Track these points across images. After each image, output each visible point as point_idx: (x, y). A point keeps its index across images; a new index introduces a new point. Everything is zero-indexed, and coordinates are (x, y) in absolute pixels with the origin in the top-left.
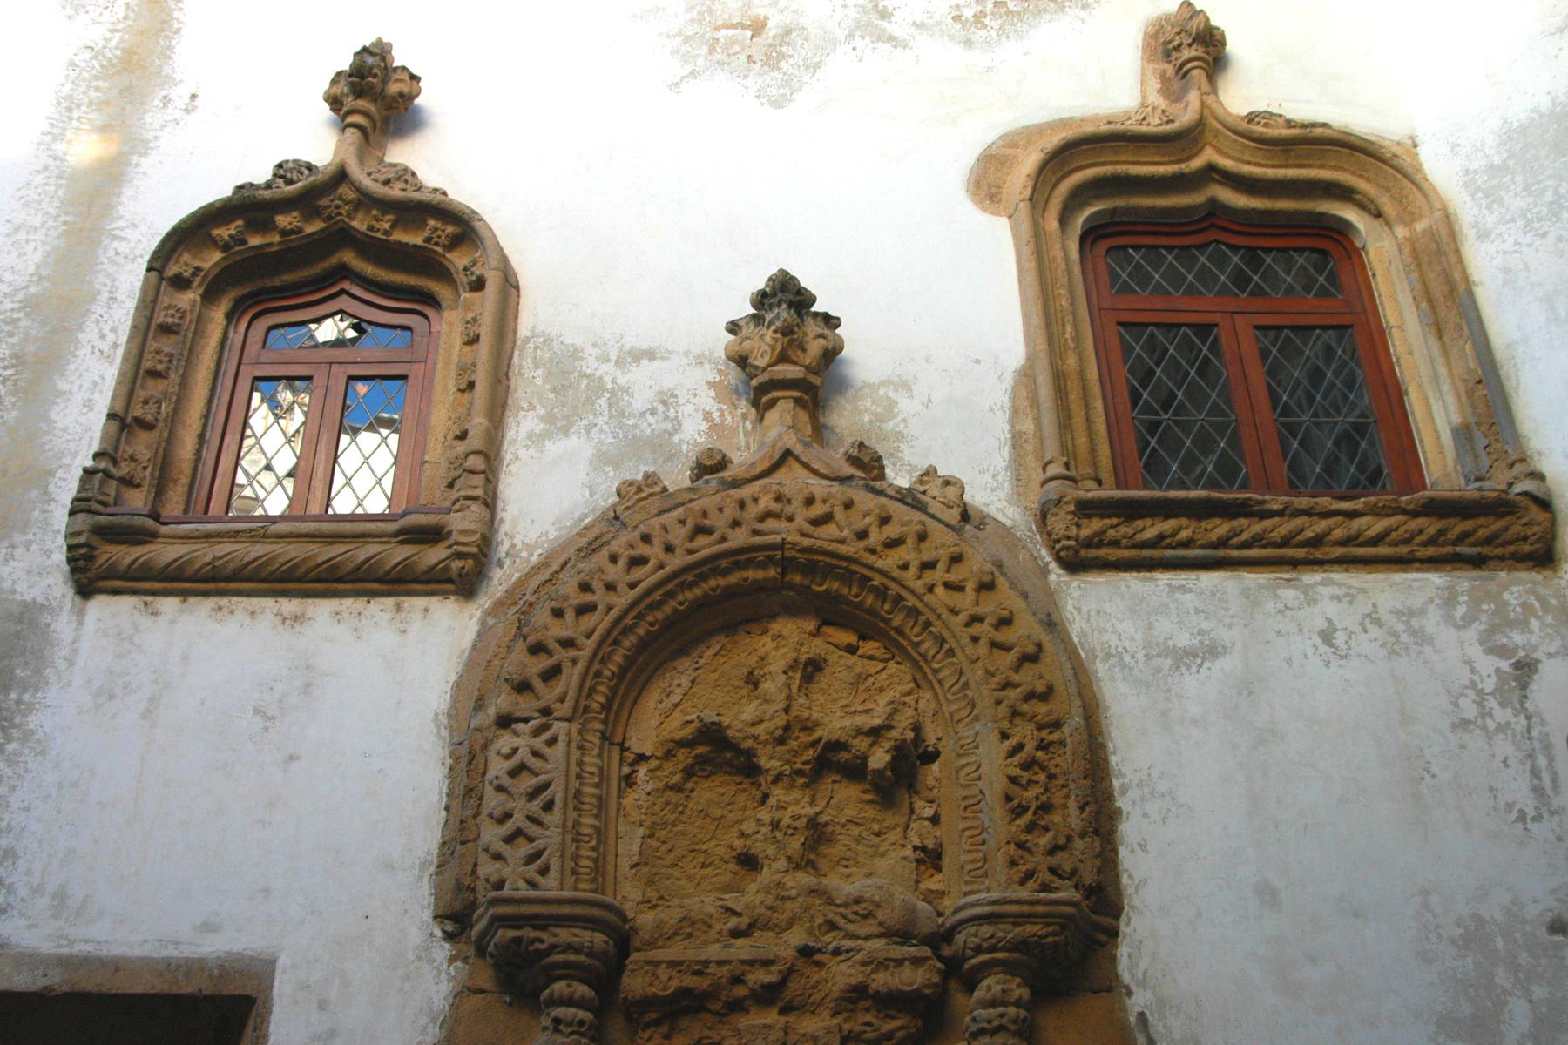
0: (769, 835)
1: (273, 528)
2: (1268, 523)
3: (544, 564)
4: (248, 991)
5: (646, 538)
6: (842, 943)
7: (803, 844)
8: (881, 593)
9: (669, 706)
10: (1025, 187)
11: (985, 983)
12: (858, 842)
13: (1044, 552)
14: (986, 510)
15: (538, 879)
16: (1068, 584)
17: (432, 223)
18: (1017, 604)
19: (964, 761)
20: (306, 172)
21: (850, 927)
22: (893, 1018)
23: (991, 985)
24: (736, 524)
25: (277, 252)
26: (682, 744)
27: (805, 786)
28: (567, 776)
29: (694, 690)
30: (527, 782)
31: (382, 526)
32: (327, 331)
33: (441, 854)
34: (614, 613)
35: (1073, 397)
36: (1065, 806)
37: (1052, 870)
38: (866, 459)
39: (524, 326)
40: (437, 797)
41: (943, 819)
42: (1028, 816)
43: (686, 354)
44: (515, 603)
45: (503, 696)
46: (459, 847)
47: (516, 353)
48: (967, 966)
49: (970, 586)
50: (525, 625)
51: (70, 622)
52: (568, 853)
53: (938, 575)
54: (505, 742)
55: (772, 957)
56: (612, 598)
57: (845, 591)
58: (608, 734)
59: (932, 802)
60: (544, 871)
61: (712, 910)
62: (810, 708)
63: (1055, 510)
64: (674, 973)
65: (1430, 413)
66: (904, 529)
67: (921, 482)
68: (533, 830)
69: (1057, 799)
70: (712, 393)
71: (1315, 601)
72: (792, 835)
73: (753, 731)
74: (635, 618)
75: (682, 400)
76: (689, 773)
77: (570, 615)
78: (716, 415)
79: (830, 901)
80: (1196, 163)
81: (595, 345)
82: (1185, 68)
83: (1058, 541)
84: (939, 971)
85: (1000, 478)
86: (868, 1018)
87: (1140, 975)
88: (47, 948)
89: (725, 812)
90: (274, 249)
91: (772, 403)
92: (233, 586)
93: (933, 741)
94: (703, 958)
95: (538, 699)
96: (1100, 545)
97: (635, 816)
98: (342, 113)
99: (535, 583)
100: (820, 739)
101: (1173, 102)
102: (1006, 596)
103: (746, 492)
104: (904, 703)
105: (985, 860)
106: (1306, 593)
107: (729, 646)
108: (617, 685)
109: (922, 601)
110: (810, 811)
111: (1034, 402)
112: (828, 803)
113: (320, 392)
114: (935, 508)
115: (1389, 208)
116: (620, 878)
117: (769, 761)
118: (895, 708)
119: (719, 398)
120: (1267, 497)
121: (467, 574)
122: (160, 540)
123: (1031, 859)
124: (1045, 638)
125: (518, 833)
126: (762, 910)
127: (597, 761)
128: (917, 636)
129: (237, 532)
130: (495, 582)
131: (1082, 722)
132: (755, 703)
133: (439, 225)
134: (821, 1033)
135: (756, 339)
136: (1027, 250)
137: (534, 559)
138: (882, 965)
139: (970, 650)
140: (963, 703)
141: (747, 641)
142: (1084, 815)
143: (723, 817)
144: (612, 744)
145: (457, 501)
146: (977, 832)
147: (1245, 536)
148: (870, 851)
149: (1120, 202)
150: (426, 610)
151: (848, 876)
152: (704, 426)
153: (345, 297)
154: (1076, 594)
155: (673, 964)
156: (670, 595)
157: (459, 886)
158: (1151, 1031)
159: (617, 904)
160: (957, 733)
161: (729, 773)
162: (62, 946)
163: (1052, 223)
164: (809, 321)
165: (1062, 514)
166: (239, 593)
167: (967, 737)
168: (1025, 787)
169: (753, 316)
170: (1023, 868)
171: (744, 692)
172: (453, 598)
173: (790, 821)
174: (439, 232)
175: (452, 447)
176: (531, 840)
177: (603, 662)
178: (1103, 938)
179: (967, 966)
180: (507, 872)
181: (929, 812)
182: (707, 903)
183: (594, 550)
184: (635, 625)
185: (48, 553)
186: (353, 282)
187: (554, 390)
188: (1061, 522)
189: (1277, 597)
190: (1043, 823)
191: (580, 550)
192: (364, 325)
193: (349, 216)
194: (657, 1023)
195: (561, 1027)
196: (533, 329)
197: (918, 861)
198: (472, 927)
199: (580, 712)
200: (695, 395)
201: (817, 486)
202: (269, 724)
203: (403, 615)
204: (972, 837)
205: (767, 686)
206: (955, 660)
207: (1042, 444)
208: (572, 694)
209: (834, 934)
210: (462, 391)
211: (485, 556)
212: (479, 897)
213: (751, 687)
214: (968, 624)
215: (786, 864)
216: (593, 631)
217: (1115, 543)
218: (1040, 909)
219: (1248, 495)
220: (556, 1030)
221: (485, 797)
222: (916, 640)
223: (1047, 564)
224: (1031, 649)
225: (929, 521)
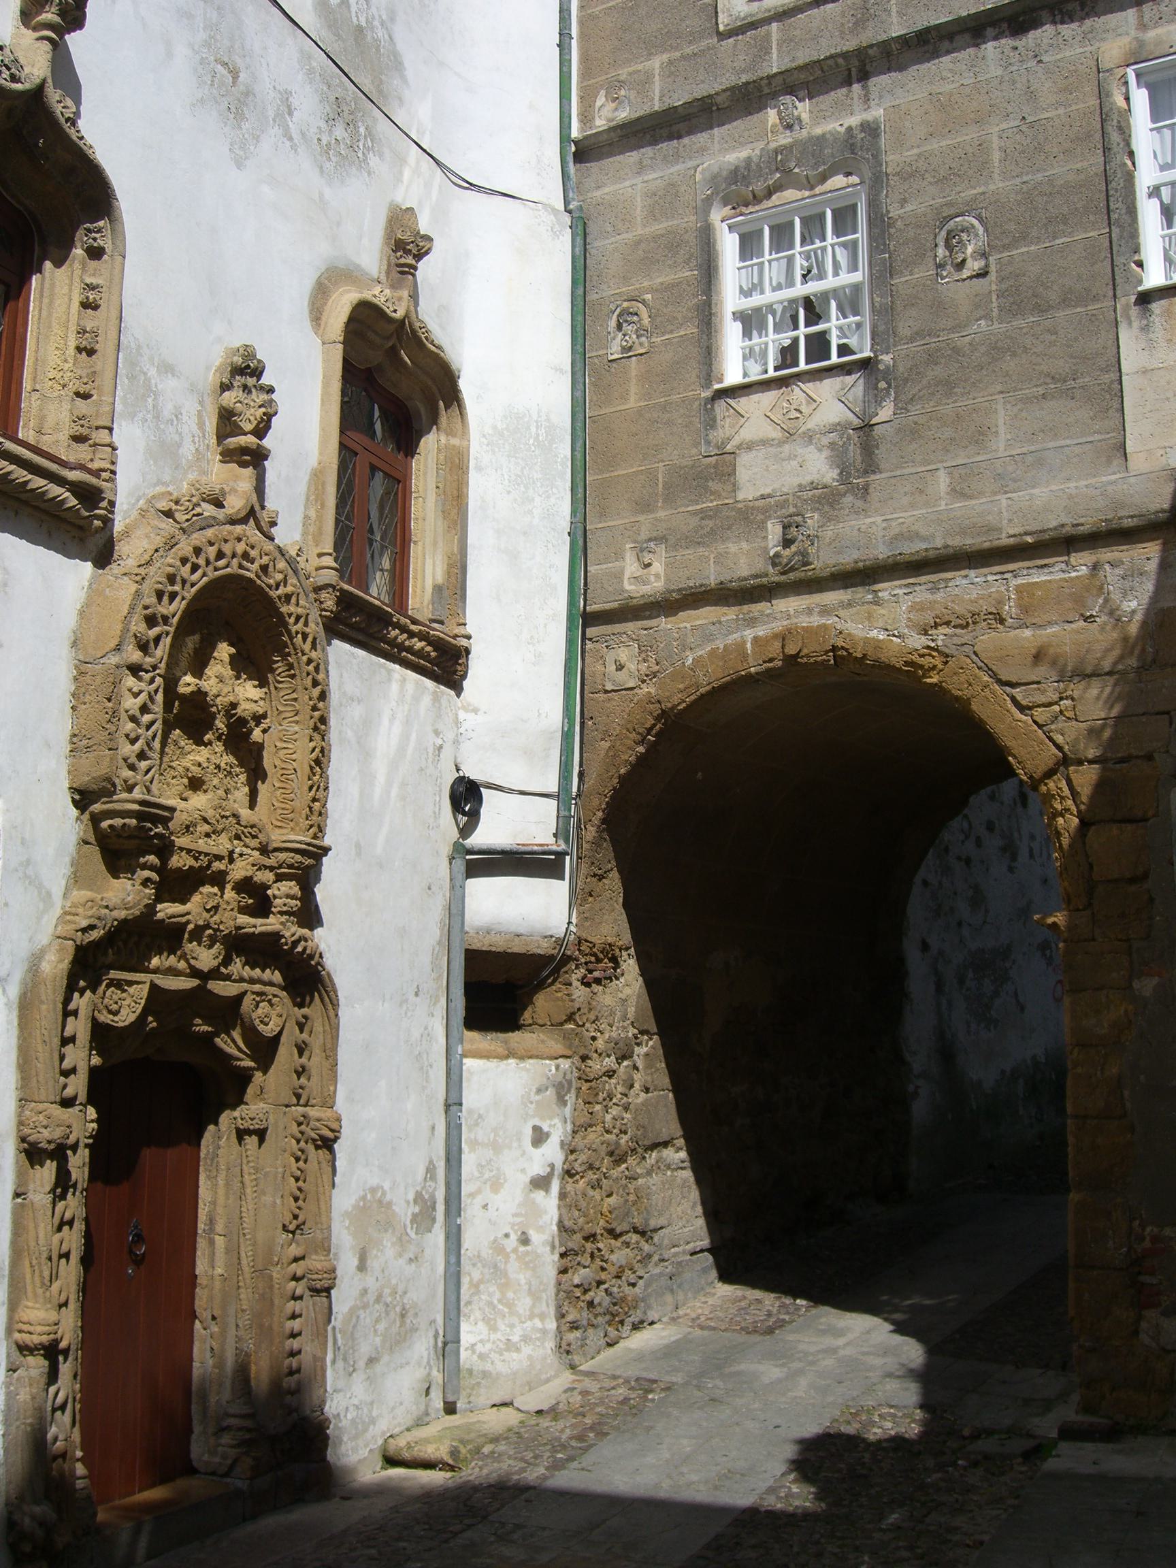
78: (197, 439)
79: (238, 823)
155: (189, 851)
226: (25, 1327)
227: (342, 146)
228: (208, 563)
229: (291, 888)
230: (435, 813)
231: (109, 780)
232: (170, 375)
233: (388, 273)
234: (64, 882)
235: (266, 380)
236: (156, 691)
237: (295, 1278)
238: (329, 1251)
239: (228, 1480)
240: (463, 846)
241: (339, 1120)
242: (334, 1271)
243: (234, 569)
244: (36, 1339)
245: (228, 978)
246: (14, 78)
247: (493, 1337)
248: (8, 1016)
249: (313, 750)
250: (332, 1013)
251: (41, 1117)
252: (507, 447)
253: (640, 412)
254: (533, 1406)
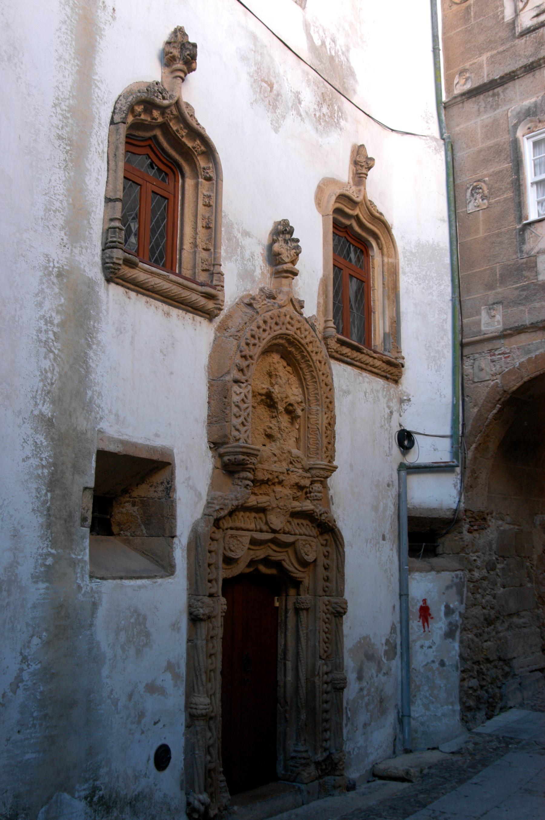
4: (170, 461)
8: (303, 357)
17: (198, 142)
51: (104, 293)
57: (295, 352)
65: (379, 323)
80: (356, 213)
88: (116, 436)
90: (147, 123)
92: (154, 295)
114: (317, 332)
115: (385, 250)
122: (138, 268)
133: (200, 144)
134: (289, 495)
152: (260, 272)
155: (267, 470)
162: (119, 435)
185: (93, 255)
195: (248, 487)
226: (194, 706)
227: (326, 117)
228: (271, 328)
229: (318, 488)
230: (389, 448)
231: (226, 436)
232: (248, 237)
233: (353, 178)
234: (207, 489)
235: (294, 236)
236: (248, 392)
237: (327, 683)
238: (343, 669)
239: (294, 784)
240: (405, 464)
241: (346, 603)
242: (345, 679)
243: (284, 331)
244: (199, 712)
245: (288, 533)
246: (164, 98)
247: (428, 713)
248: (182, 553)
249: (328, 417)
250: (341, 549)
251: (200, 603)
252: (418, 261)
253: (485, 238)
254: (448, 749)
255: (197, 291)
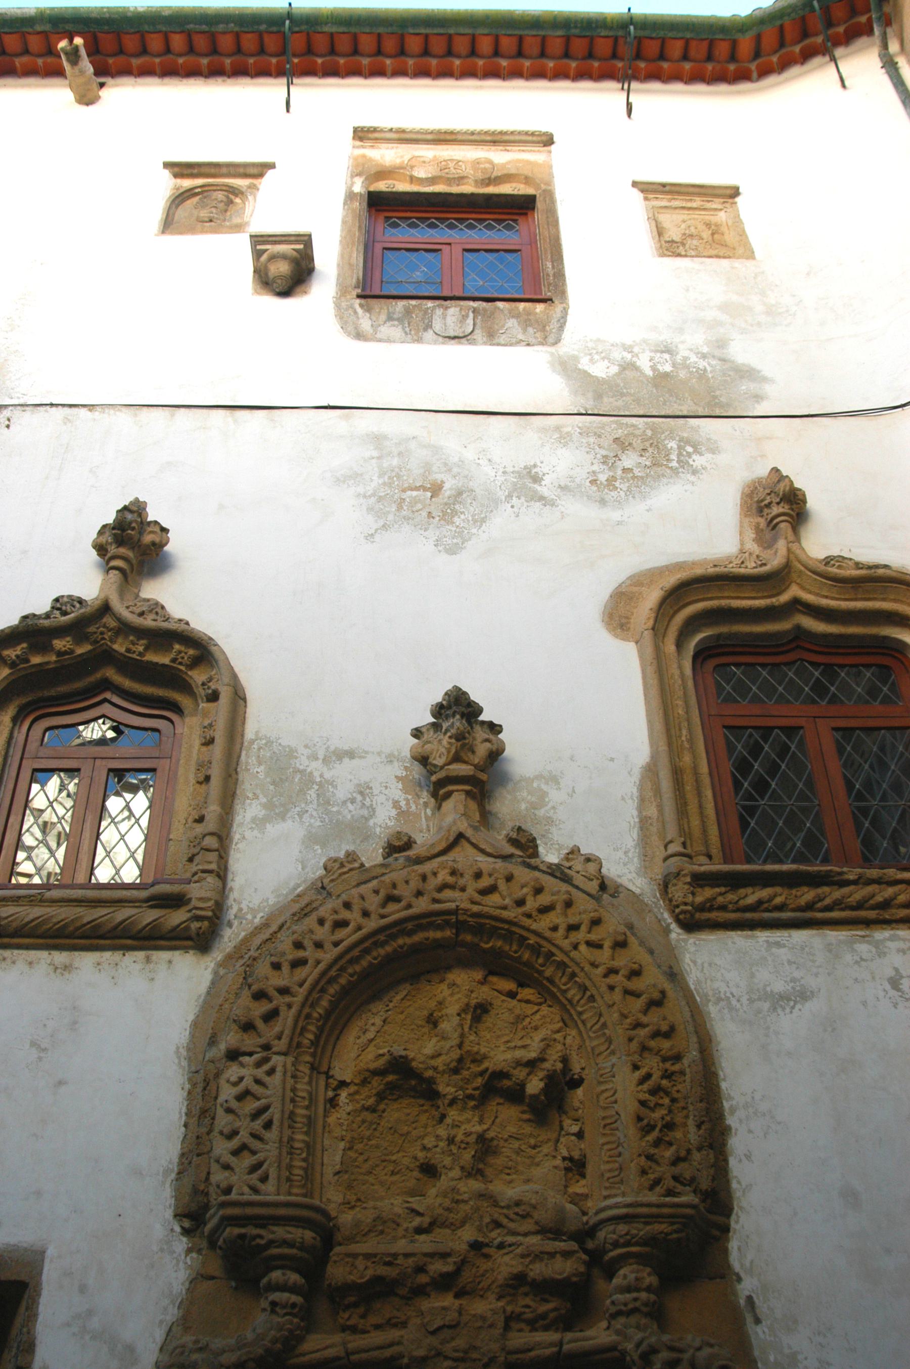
0: (445, 1149)
1: (48, 894)
2: (846, 890)
3: (265, 925)
4: (23, 1277)
5: (347, 905)
6: (505, 1239)
7: (473, 1156)
8: (536, 950)
9: (365, 1041)
10: (649, 618)
11: (622, 1272)
12: (518, 1153)
13: (666, 915)
14: (619, 880)
15: (259, 1185)
16: (685, 941)
17: (177, 647)
18: (644, 958)
19: (603, 1088)
20: (78, 605)
21: (512, 1225)
22: (546, 1301)
23: (626, 1274)
24: (419, 893)
25: (55, 669)
26: (376, 1073)
27: (475, 1107)
28: (283, 1099)
29: (386, 1028)
30: (251, 1105)
31: (135, 893)
32: (96, 731)
33: (181, 1163)
34: (322, 967)
35: (688, 788)
36: (685, 1125)
37: (675, 1178)
38: (523, 841)
39: (251, 730)
40: (177, 1116)
41: (586, 1135)
42: (655, 1134)
43: (379, 754)
44: (242, 957)
45: (232, 1033)
46: (195, 1159)
47: (244, 753)
48: (606, 1258)
49: (607, 944)
50: (250, 976)
52: (284, 1164)
53: (581, 935)
54: (233, 1071)
55: (448, 1250)
56: (320, 954)
57: (507, 948)
58: (316, 1065)
59: (577, 1120)
60: (264, 1179)
61: (400, 1211)
62: (478, 1044)
63: (675, 881)
64: (369, 1264)
66: (555, 897)
67: (568, 859)
68: (255, 1144)
69: (678, 1119)
70: (400, 786)
71: (885, 954)
72: (465, 1148)
73: (433, 1063)
74: (338, 970)
75: (376, 792)
76: (381, 1097)
77: (286, 968)
78: (403, 803)
79: (496, 1204)
80: (784, 598)
81: (306, 746)
82: (775, 522)
83: (678, 906)
84: (584, 1262)
85: (630, 855)
86: (527, 1301)
87: (748, 1264)
89: (410, 1129)
91: (448, 795)
93: (579, 1070)
94: (393, 1251)
95: (260, 1036)
96: (711, 909)
97: (338, 1132)
98: (107, 558)
99: (257, 941)
100: (487, 1069)
101: (765, 548)
102: (636, 953)
103: (427, 867)
104: (555, 1040)
105: (621, 1169)
106: (877, 947)
107: (413, 993)
108: (324, 1025)
109: (569, 956)
110: (479, 1128)
111: (657, 792)
112: (493, 1122)
113: (87, 781)
114: (579, 880)
116: (325, 1184)
117: (446, 1088)
118: (548, 1043)
119: (405, 790)
120: (845, 869)
121: (204, 933)
123: (658, 1169)
124: (667, 986)
125: (244, 1147)
126: (440, 1211)
127: (308, 1088)
128: (564, 984)
129: (19, 897)
130: (226, 939)
131: (698, 1055)
132: (434, 1040)
133: (183, 649)
135: (435, 743)
136: (651, 670)
137: (257, 921)
138: (538, 1256)
139: (607, 997)
140: (603, 1040)
141: (428, 987)
142: (701, 1132)
143: (408, 1133)
144: (319, 1073)
145: (195, 874)
146: (614, 1146)
147: (828, 901)
148: (527, 1161)
149: (724, 629)
150: (170, 962)
151: (511, 1182)
152: (394, 812)
153: (107, 705)
154: (692, 949)
155: (368, 1256)
156: (367, 951)
157: (195, 1191)
158: (758, 1311)
159: (323, 1206)
160: (597, 1064)
161: (414, 1097)
163: (670, 647)
164: (477, 728)
165: (680, 885)
166: (19, 947)
167: (605, 1068)
168: (652, 1110)
169: (433, 725)
170: (652, 1176)
171: (426, 1030)
172: (191, 952)
173: (463, 1137)
174: (183, 654)
175: (192, 829)
176: (254, 1153)
177: (312, 1006)
178: (717, 1233)
179: (606, 1258)
180: (234, 1179)
181: (575, 1129)
182: (395, 1204)
183: (306, 915)
184: (338, 976)
186: (113, 693)
187: (273, 783)
188: (679, 892)
189: (854, 950)
190: (667, 1139)
191: (294, 915)
192: (122, 727)
193: (111, 641)
194: (355, 1305)
195: (278, 1309)
196: (257, 733)
197: (567, 1170)
198: (205, 1224)
199: (294, 1048)
200: (386, 787)
201: (485, 863)
202: (42, 1055)
203: (152, 966)
204: (610, 1150)
205: (444, 1026)
206: (595, 1004)
207: (664, 826)
208: (287, 1032)
209: (498, 1231)
210: (200, 783)
211: (218, 918)
212: (212, 1200)
213: (431, 1026)
214: (606, 976)
215: (460, 1173)
216: (304, 981)
217: (723, 908)
218: (666, 1211)
219: (829, 868)
220: (273, 1311)
221: (217, 1117)
222: (564, 988)
223: (669, 925)
224: (656, 995)
225: (574, 891)
255: (130, 902)
